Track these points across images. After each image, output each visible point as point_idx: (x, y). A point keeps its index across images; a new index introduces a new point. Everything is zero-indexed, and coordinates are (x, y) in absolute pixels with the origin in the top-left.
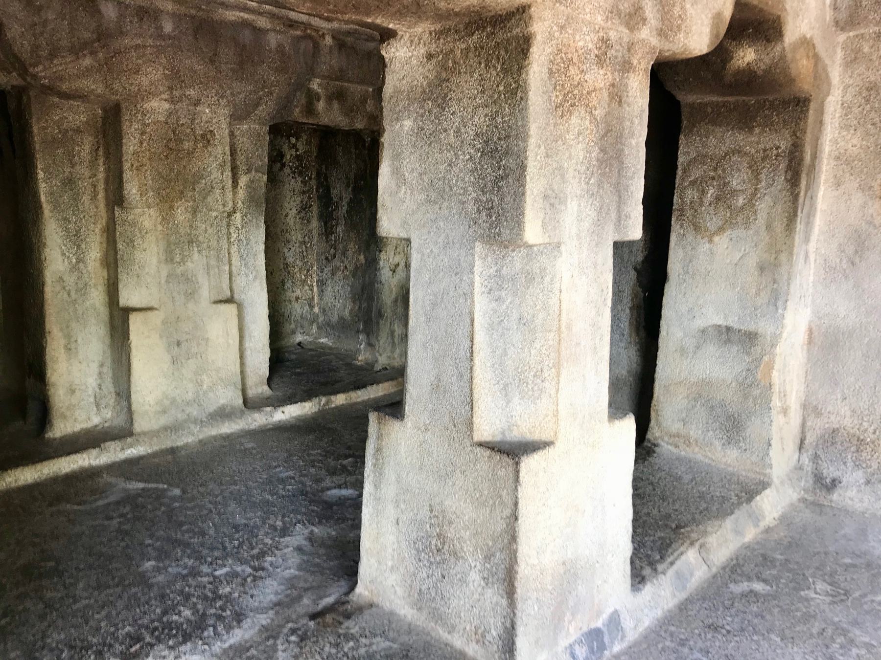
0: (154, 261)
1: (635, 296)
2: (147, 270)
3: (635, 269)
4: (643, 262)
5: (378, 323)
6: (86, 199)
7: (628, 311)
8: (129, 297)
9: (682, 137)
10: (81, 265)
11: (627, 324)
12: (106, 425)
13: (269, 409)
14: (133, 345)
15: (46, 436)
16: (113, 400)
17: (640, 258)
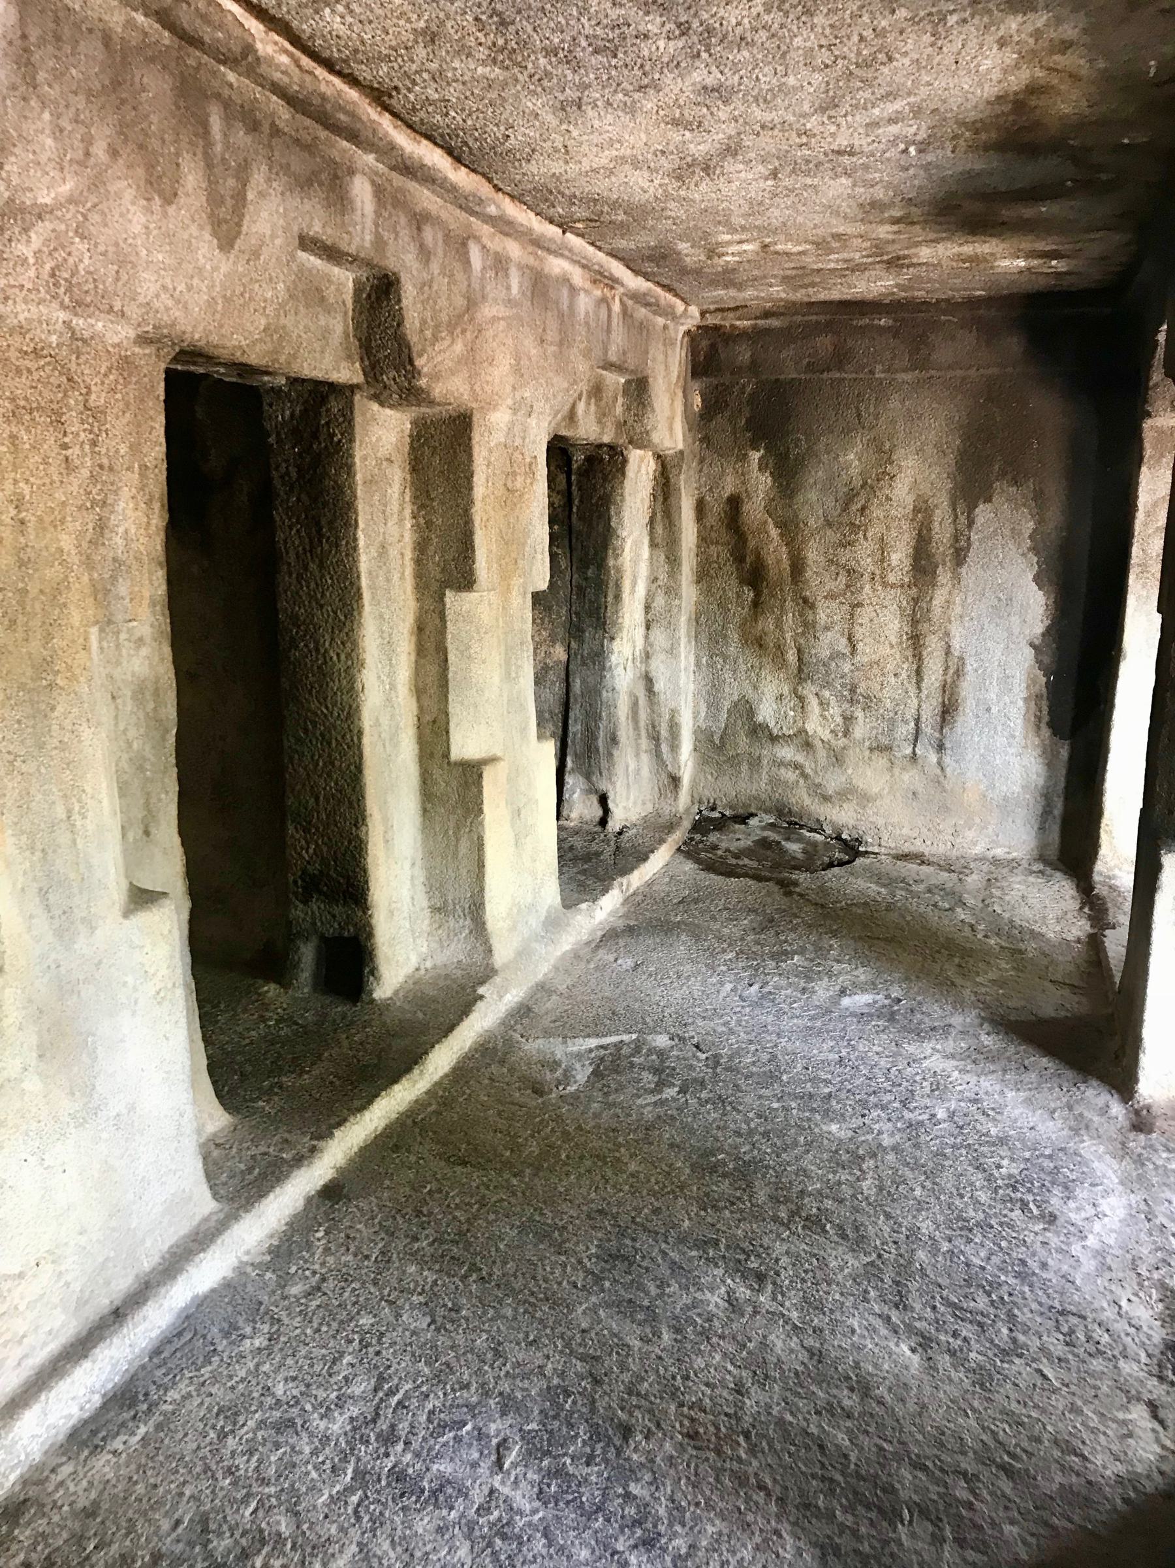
0: (496, 680)
1: (1033, 681)
2: (487, 694)
3: (1032, 645)
4: (1043, 635)
5: (610, 755)
6: (396, 577)
7: (1021, 703)
8: (466, 743)
9: (1144, 469)
10: (393, 694)
11: (1020, 721)
12: (429, 964)
13: (584, 906)
14: (487, 823)
15: (376, 995)
16: (427, 922)
17: (1039, 629)
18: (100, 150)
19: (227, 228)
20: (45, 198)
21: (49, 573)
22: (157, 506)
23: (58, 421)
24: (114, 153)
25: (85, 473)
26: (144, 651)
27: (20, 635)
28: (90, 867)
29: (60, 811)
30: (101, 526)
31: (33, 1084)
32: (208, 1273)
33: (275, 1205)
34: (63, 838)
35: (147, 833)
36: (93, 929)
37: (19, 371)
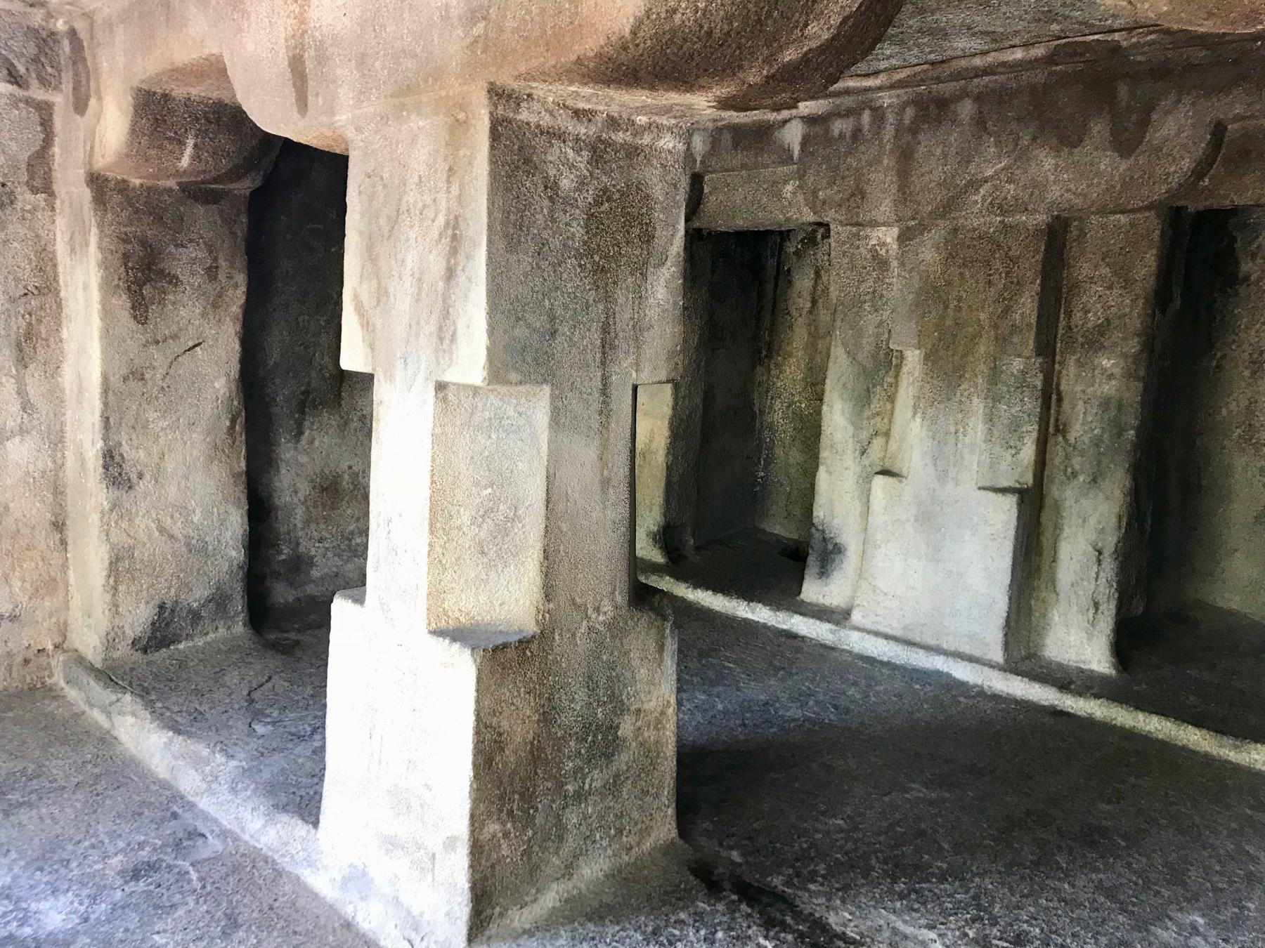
18: (1025, 141)
19: (1124, 144)
20: (989, 172)
21: (971, 329)
22: (1141, 302)
23: (987, 263)
24: (1034, 139)
25: (1000, 286)
26: (1113, 382)
27: (950, 353)
28: (962, 458)
29: (952, 429)
30: (1007, 310)
31: (909, 528)
32: (962, 672)
33: (1022, 685)
34: (952, 440)
35: (1094, 480)
36: (957, 485)
37: (969, 247)
